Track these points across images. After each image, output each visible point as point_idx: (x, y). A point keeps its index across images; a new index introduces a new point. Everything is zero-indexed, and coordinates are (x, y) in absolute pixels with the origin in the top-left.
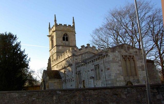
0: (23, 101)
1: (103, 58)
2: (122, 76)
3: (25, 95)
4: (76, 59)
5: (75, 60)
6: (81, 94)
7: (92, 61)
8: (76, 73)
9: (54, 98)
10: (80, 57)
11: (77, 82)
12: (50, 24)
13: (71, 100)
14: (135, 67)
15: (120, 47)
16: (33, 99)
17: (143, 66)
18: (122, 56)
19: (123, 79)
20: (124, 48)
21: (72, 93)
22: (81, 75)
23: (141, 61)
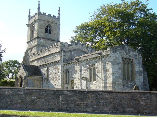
0: (18, 100)
1: (102, 58)
2: (121, 79)
3: (22, 93)
4: (65, 56)
5: (63, 56)
6: (93, 96)
7: (87, 60)
8: (63, 72)
9: (61, 98)
10: (69, 53)
11: (63, 82)
12: (59, 9)
13: (82, 103)
14: (132, 71)
15: (121, 47)
16: (33, 98)
17: (140, 71)
18: (123, 58)
19: (121, 83)
20: (125, 50)
21: (83, 95)
22: (70, 74)
23: (139, 65)
